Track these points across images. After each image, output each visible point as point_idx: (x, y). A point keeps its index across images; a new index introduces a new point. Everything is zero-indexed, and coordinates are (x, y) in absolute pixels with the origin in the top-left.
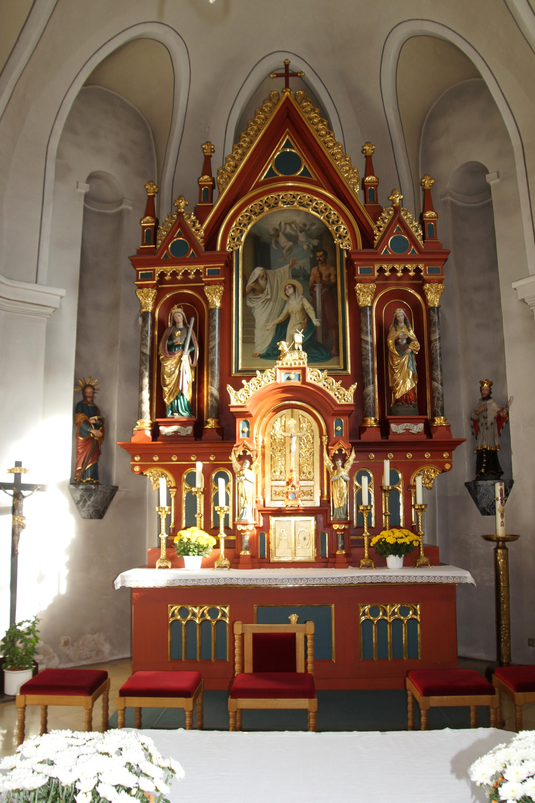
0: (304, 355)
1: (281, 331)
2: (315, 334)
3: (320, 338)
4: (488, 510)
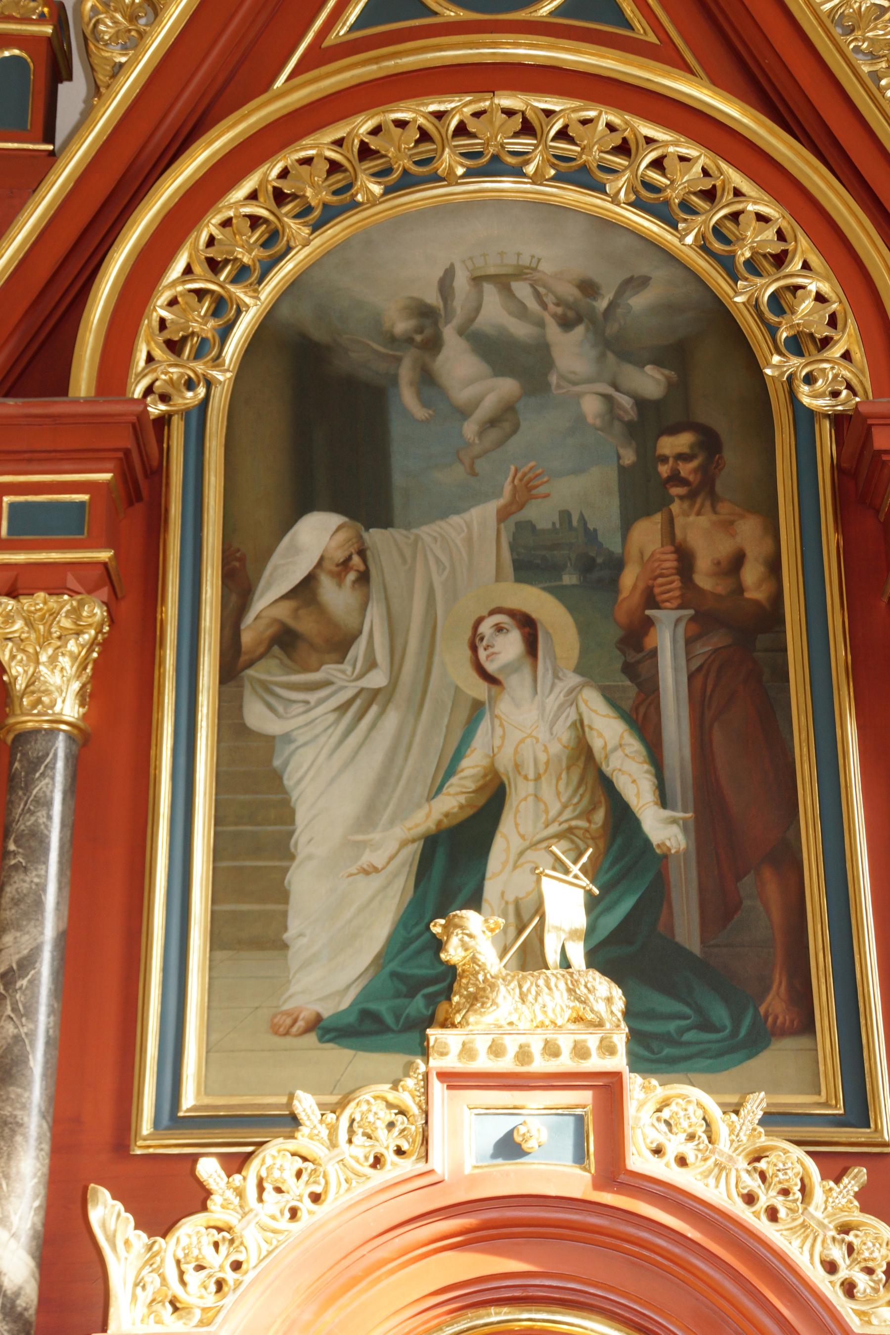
0: (607, 996)
1: (453, 864)
2: (656, 896)
3: (686, 927)
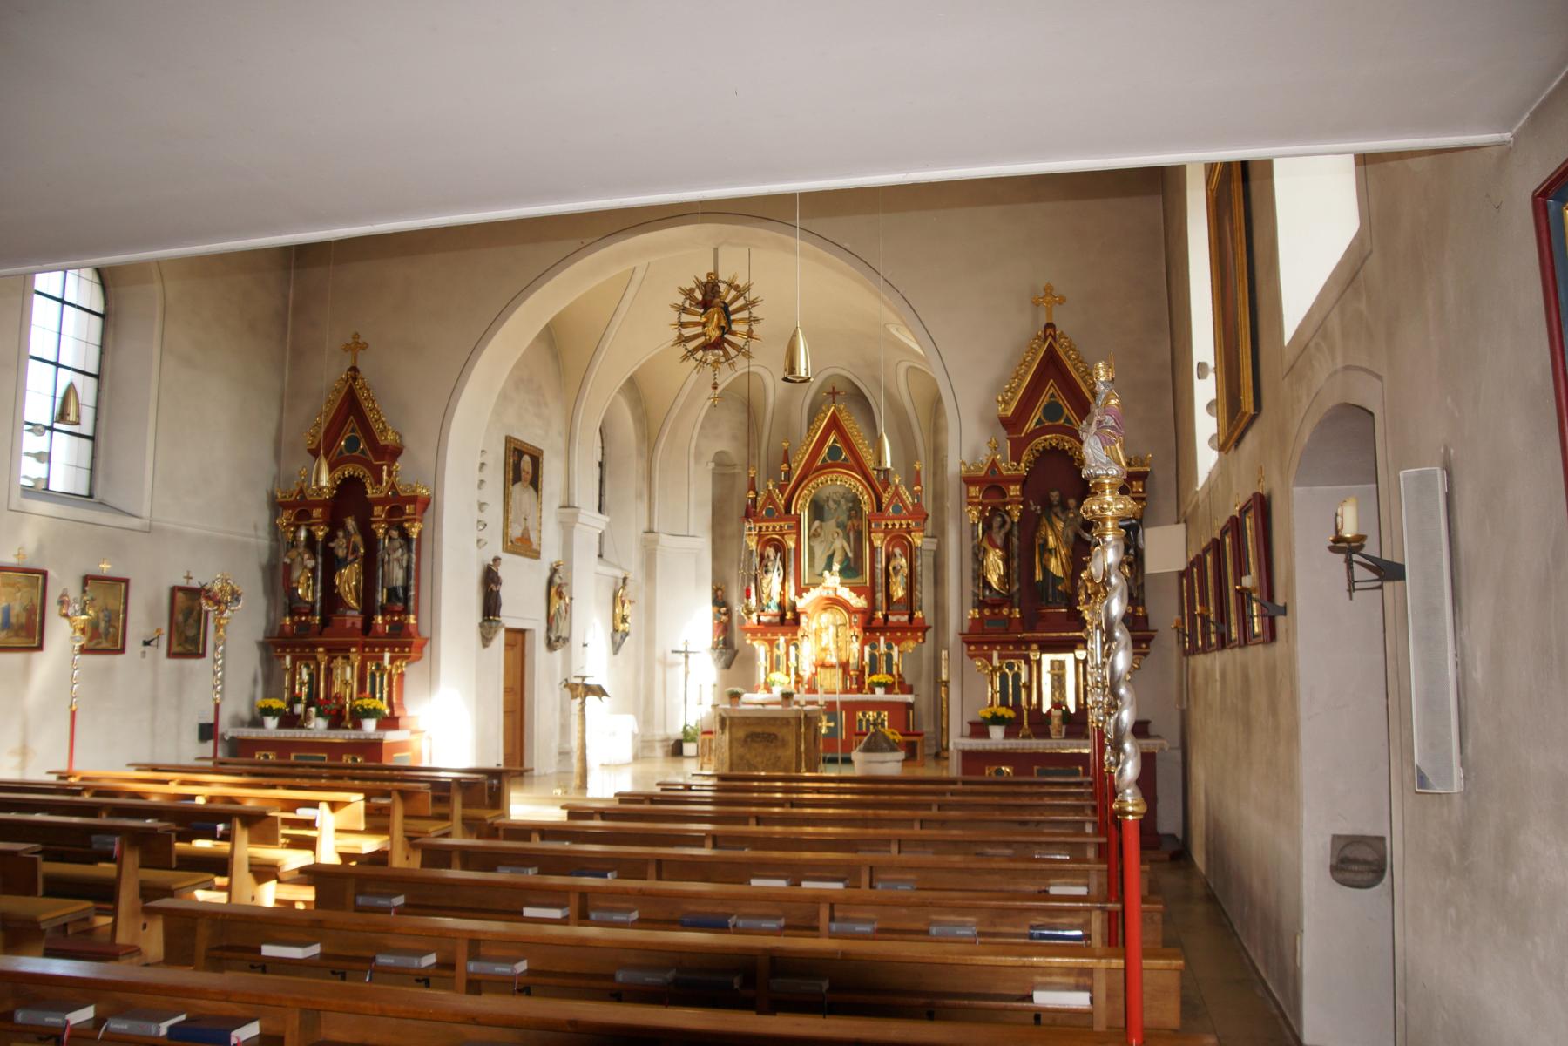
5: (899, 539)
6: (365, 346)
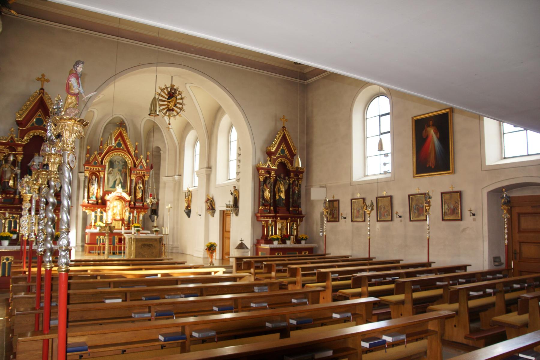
4: (153, 221)
5: (141, 178)
6: (48, 81)
